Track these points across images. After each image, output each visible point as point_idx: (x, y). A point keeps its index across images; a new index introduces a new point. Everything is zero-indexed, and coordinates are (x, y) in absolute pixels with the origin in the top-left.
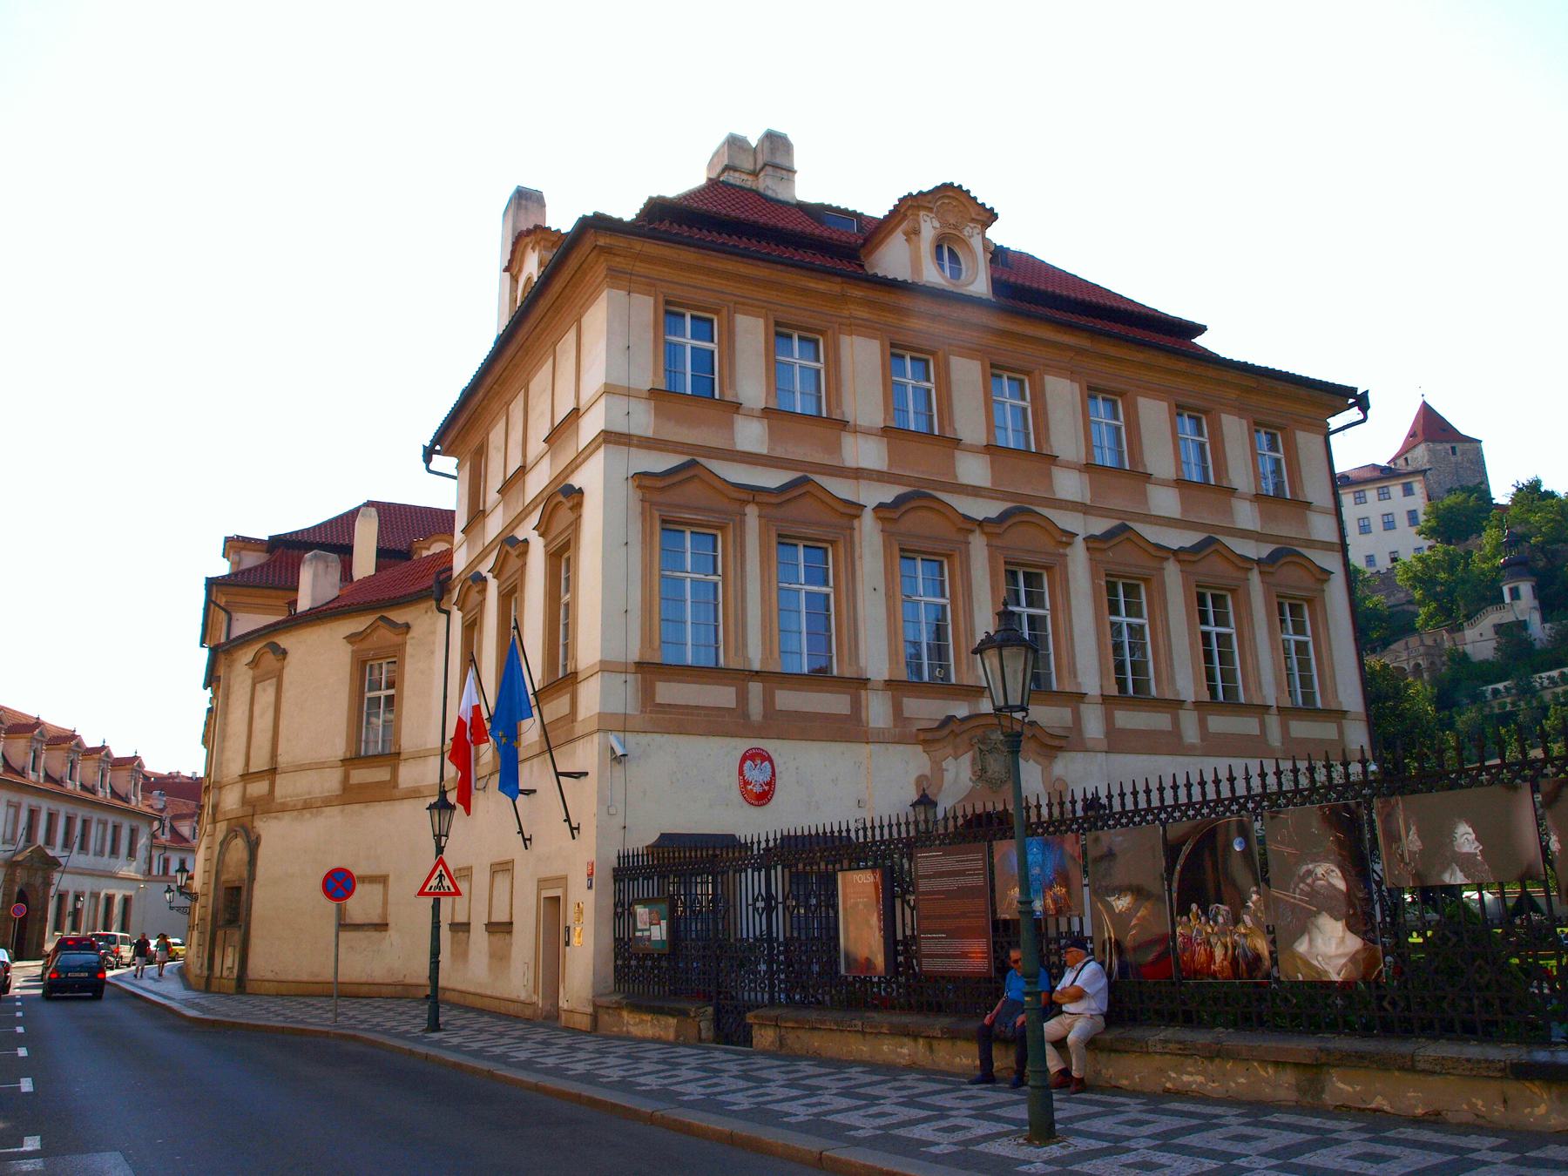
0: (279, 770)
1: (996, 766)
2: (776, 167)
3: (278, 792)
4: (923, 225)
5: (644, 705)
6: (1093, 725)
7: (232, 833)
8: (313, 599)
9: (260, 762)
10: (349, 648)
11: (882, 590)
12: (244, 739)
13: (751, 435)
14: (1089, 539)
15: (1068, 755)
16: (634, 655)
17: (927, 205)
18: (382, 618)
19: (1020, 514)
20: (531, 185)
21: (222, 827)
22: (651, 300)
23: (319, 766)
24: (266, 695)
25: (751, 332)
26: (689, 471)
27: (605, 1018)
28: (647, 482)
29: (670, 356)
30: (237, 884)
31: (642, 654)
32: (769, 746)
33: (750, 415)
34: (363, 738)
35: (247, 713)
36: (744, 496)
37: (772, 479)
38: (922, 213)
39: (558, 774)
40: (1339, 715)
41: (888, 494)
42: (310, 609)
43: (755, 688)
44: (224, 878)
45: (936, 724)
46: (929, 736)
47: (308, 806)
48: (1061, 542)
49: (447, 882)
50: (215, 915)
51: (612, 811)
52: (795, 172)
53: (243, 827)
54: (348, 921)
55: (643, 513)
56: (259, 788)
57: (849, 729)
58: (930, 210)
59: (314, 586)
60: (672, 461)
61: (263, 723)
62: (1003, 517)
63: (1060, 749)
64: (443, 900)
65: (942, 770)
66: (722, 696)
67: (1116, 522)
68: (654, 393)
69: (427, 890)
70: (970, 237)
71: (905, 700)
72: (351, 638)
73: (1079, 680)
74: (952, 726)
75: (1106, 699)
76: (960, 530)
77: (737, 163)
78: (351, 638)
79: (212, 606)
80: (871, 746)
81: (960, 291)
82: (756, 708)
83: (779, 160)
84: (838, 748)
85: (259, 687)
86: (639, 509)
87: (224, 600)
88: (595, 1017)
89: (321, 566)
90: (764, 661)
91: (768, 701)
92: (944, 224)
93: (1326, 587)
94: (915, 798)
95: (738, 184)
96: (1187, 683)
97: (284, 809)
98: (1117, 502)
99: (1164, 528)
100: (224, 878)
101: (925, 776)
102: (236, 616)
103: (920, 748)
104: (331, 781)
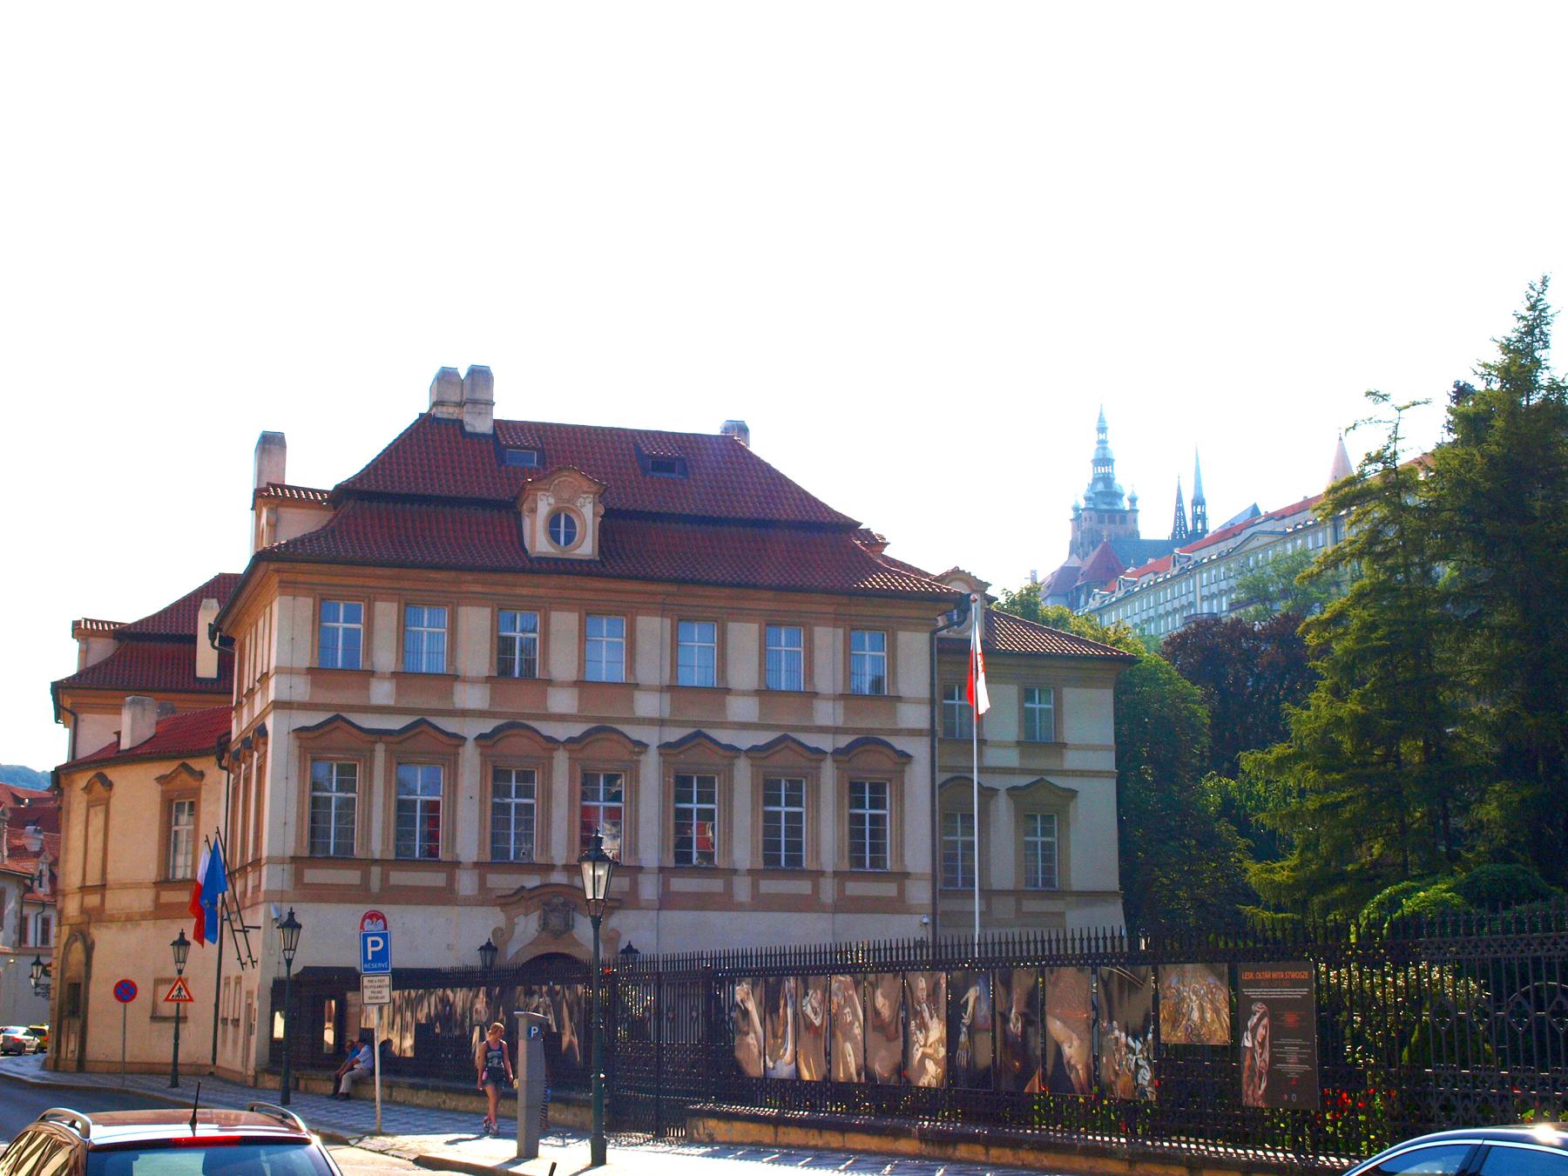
0: (108, 887)
1: (555, 921)
2: (475, 402)
3: (108, 905)
4: (540, 504)
6: (649, 888)
8: (132, 741)
9: (93, 879)
10: (159, 788)
11: (477, 798)
13: (382, 692)
14: (665, 748)
15: (621, 912)
16: (290, 852)
18: (184, 766)
19: (601, 731)
20: (273, 428)
21: (66, 930)
22: (310, 601)
23: (137, 885)
24: (97, 821)
26: (337, 721)
27: (260, 1079)
28: (304, 735)
29: (323, 640)
33: (383, 677)
35: (83, 832)
36: (373, 738)
37: (396, 723)
38: (539, 493)
39: (233, 931)
40: (903, 876)
41: (487, 726)
42: (130, 749)
44: (67, 975)
45: (511, 892)
46: (502, 901)
47: (130, 919)
48: (634, 752)
49: (184, 993)
50: (61, 1008)
51: (272, 952)
52: (494, 404)
54: (158, 1014)
55: (300, 757)
56: (93, 900)
57: (444, 896)
59: (133, 730)
60: (321, 717)
62: (587, 734)
64: (182, 1005)
66: (351, 877)
67: (690, 731)
68: (310, 671)
71: (488, 876)
72: (161, 780)
73: (640, 856)
75: (661, 869)
77: (446, 397)
78: (161, 780)
79: (62, 710)
81: (566, 557)
83: (478, 395)
84: (432, 909)
85: (92, 810)
86: (296, 753)
88: (256, 1078)
89: (139, 709)
90: (382, 851)
91: (385, 878)
92: (559, 499)
94: (484, 944)
96: (743, 851)
97: (112, 919)
98: (694, 714)
100: (67, 975)
102: (81, 717)
103: (498, 909)
104: (143, 900)
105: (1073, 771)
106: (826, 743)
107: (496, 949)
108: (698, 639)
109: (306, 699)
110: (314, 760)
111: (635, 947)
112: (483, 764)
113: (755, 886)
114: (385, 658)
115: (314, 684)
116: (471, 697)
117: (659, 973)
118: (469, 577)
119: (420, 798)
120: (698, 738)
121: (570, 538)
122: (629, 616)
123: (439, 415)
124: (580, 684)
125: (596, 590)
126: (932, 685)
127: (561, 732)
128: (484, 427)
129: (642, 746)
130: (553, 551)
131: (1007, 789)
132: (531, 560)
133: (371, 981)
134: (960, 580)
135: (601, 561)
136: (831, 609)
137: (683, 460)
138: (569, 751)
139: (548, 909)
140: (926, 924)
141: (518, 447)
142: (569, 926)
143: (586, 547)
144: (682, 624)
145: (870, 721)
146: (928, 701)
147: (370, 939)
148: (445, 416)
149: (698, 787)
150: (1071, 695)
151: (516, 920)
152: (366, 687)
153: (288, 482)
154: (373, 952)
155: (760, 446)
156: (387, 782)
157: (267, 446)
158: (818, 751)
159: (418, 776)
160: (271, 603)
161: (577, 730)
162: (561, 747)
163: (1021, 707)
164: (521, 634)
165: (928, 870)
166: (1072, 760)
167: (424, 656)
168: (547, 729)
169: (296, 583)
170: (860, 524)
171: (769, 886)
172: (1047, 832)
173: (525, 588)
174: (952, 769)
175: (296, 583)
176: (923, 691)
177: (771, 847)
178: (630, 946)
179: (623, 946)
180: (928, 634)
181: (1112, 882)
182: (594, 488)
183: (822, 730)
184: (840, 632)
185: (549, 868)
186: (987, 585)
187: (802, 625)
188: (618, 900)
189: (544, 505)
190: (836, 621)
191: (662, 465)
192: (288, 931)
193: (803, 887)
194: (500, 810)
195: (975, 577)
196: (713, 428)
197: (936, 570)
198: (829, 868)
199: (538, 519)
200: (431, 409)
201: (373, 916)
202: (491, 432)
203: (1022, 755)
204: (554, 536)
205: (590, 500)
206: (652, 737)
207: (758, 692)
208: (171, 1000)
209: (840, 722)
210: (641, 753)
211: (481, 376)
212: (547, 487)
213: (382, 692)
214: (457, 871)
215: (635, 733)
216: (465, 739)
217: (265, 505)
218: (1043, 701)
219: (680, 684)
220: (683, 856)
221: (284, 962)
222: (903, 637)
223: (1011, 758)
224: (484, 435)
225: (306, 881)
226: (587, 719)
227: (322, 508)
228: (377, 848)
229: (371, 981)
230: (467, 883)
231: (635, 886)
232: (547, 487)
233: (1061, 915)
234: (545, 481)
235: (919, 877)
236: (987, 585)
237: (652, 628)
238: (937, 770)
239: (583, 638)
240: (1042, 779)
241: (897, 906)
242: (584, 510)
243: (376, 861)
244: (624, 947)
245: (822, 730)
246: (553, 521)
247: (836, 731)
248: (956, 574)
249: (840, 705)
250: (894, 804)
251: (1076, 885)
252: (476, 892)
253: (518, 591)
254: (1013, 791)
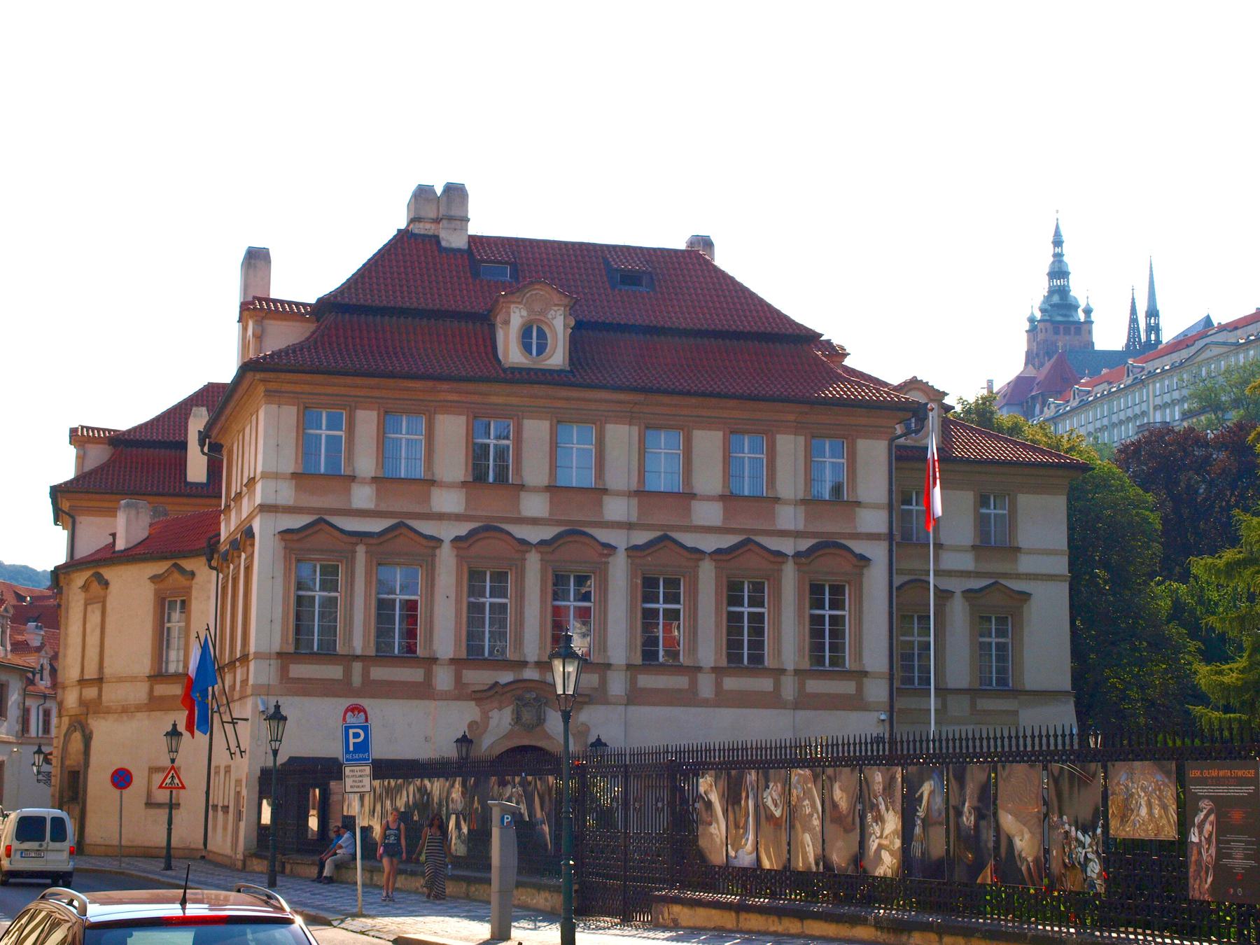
0: (105, 680)
1: (527, 716)
2: (451, 219)
5: (282, 679)
6: (617, 684)
7: (71, 728)
8: (127, 541)
9: (91, 673)
11: (453, 596)
12: (79, 649)
13: (363, 497)
14: (633, 550)
16: (276, 647)
17: (516, 300)
18: (175, 565)
19: (574, 533)
21: (66, 720)
22: (294, 410)
23: (133, 679)
24: (94, 618)
25: (367, 421)
26: (320, 524)
27: (248, 863)
28: (287, 537)
29: (306, 446)
30: (77, 769)
31: (281, 647)
32: (365, 702)
33: (363, 481)
34: (164, 659)
36: (354, 540)
37: (376, 526)
38: (512, 306)
39: (223, 722)
40: (861, 675)
41: (463, 529)
42: (125, 550)
43: (357, 667)
44: (67, 763)
45: (486, 688)
46: (479, 695)
47: (126, 711)
48: (603, 554)
49: (176, 781)
50: (61, 792)
51: (259, 743)
52: (468, 220)
53: (80, 723)
54: (153, 801)
55: (285, 557)
56: (91, 693)
57: (423, 691)
58: (519, 303)
59: (127, 531)
61: (93, 640)
63: (586, 703)
64: (174, 791)
65: (488, 718)
66: (333, 672)
67: (659, 533)
68: (295, 475)
69: (164, 785)
70: (553, 319)
71: (464, 672)
72: (154, 579)
73: (609, 654)
74: (496, 689)
75: (629, 667)
76: (517, 551)
77: (423, 214)
78: (154, 579)
79: (60, 512)
80: (437, 702)
82: (357, 680)
83: (455, 212)
84: (416, 702)
85: (89, 608)
86: (282, 554)
87: (68, 505)
88: (244, 862)
89: (133, 512)
91: (365, 674)
92: (530, 311)
93: (865, 571)
94: (460, 736)
95: (422, 232)
96: (709, 651)
97: (108, 711)
99: (703, 535)
100: (67, 763)
101: (476, 723)
102: (79, 519)
103: (473, 703)
104: (139, 693)
105: (1026, 574)
106: (787, 546)
107: (471, 742)
108: (665, 446)
109: (291, 502)
110: (298, 561)
111: (603, 741)
112: (459, 566)
113: (718, 684)
114: (366, 464)
115: (298, 488)
116: (448, 501)
117: (626, 766)
118: (445, 386)
119: (399, 597)
120: (665, 539)
121: (542, 348)
122: (598, 423)
123: (416, 231)
124: (552, 489)
125: (567, 399)
126: (890, 491)
127: (533, 535)
128: (459, 242)
129: (611, 548)
130: (527, 362)
131: (964, 592)
132: (505, 370)
133: (353, 771)
134: (918, 389)
135: (571, 371)
136: (791, 417)
137: (650, 273)
138: (541, 553)
139: (521, 704)
140: (883, 720)
141: (492, 262)
142: (541, 721)
143: (557, 358)
144: (649, 433)
145: (830, 526)
146: (887, 506)
147: (351, 731)
148: (422, 232)
149: (664, 588)
150: (1026, 501)
151: (490, 714)
152: (348, 491)
153: (273, 296)
154: (354, 743)
155: (723, 260)
156: (368, 583)
157: (253, 261)
158: (779, 554)
159: (398, 576)
160: (257, 411)
161: (548, 533)
162: (534, 549)
163: (976, 511)
164: (495, 441)
166: (1026, 564)
167: (403, 461)
168: (520, 532)
169: (280, 392)
170: (821, 335)
171: (730, 683)
172: (1001, 633)
173: (499, 396)
174: (911, 572)
175: (280, 392)
177: (733, 645)
178: (599, 740)
179: (592, 739)
180: (887, 442)
181: (1065, 683)
182: (566, 301)
183: (783, 534)
184: (801, 439)
185: (523, 664)
186: (947, 394)
187: (765, 433)
188: (588, 695)
189: (516, 317)
190: (797, 429)
191: (631, 279)
192: (274, 723)
193: (764, 684)
194: (475, 609)
195: (932, 386)
196: (678, 242)
197: (895, 379)
198: (790, 666)
199: (511, 331)
200: (408, 225)
201: (355, 709)
202: (466, 247)
203: (977, 559)
204: (527, 347)
205: (561, 312)
206: (618, 539)
207: (722, 498)
208: (164, 788)
209: (801, 527)
210: (610, 555)
211: (456, 193)
212: (519, 300)
213: (363, 497)
214: (434, 666)
215: (603, 535)
217: (251, 317)
218: (998, 506)
219: (647, 489)
220: (649, 654)
221: (271, 752)
222: (863, 445)
223: (966, 562)
224: (459, 250)
225: (291, 675)
226: (558, 523)
227: (308, 320)
228: (358, 647)
229: (353, 771)
230: (443, 679)
231: (603, 682)
232: (519, 300)
233: (1016, 713)
234: (518, 294)
235: (877, 676)
236: (945, 394)
237: (620, 436)
238: (894, 571)
239: (554, 446)
240: (996, 583)
241: (856, 703)
242: (555, 322)
243: (357, 656)
244: (594, 741)
245: (783, 534)
246: (526, 333)
247: (797, 534)
248: (914, 384)
249: (801, 510)
250: (853, 607)
251: (1030, 684)
252: (452, 688)
253: (494, 399)
254: (968, 593)
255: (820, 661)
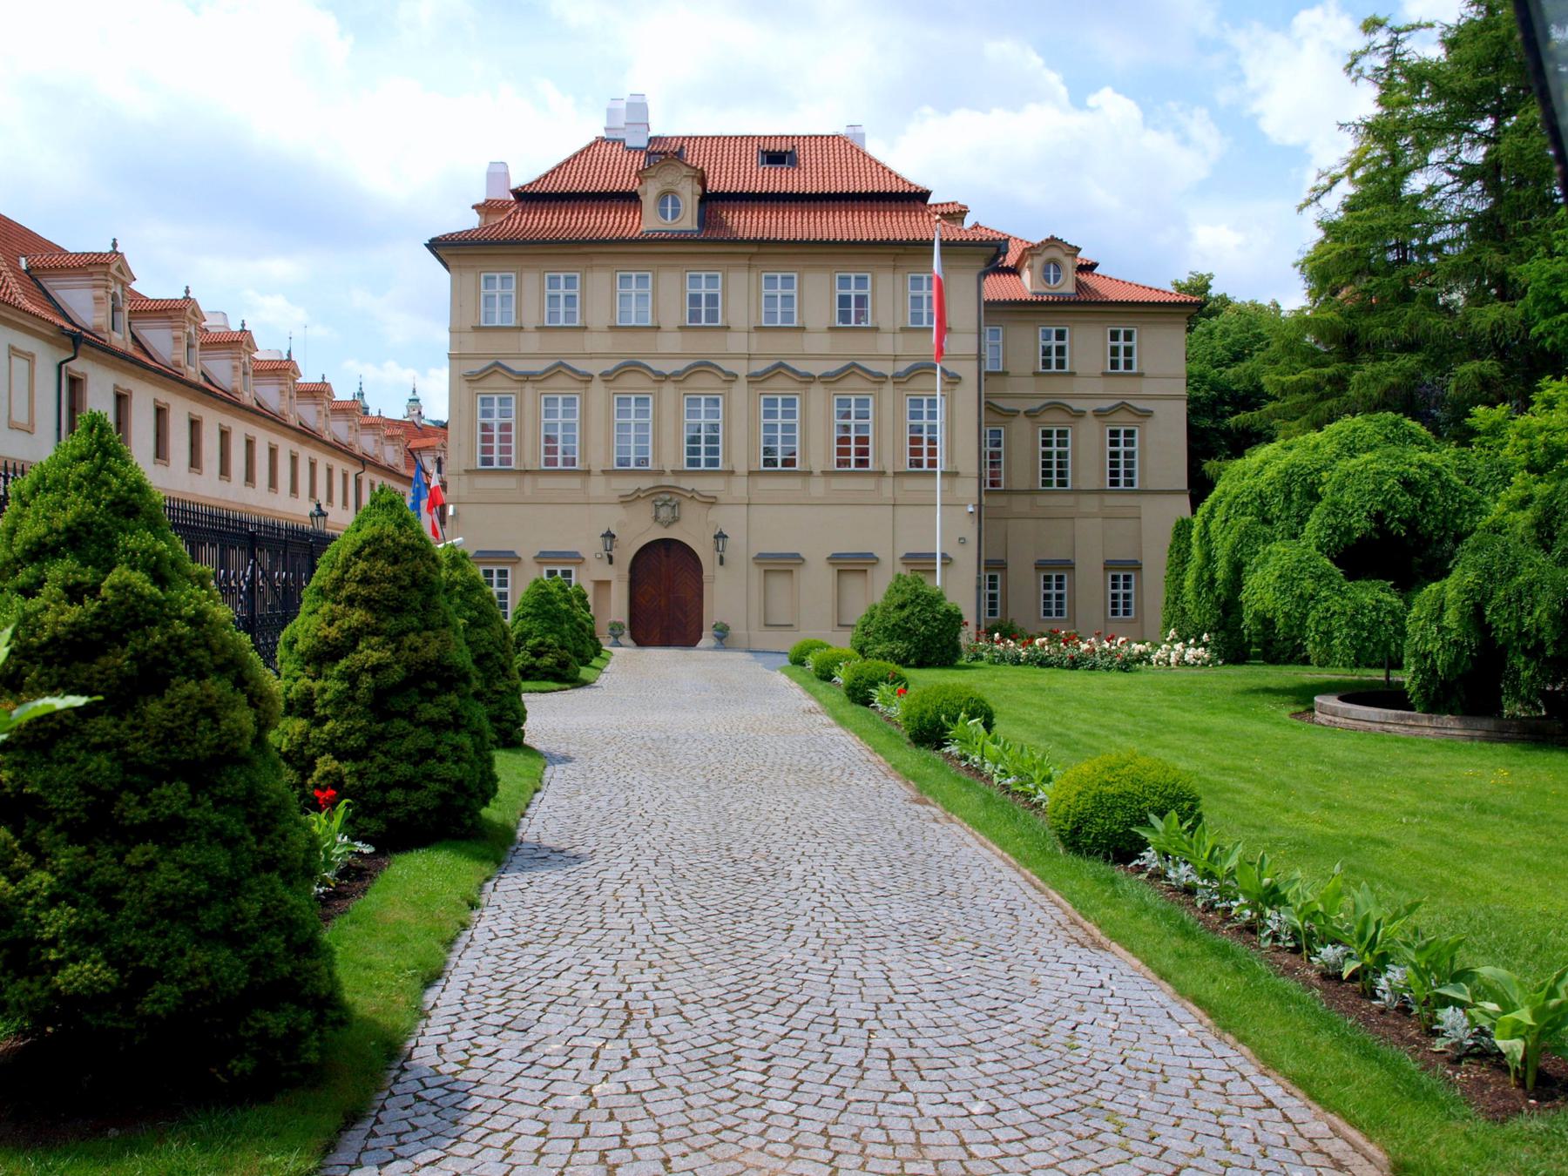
37: (539, 366)
62: (690, 368)
63: (712, 503)
75: (751, 473)
107: (614, 536)
121: (675, 214)
143: (687, 220)
165: (975, 471)
176: (972, 324)
186: (1078, 250)
216: (592, 376)
223: (1099, 386)
236: (1078, 250)
247: (896, 358)
248: (1053, 242)
255: (1114, 483)
